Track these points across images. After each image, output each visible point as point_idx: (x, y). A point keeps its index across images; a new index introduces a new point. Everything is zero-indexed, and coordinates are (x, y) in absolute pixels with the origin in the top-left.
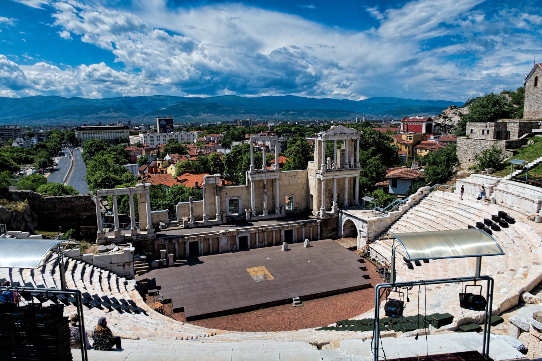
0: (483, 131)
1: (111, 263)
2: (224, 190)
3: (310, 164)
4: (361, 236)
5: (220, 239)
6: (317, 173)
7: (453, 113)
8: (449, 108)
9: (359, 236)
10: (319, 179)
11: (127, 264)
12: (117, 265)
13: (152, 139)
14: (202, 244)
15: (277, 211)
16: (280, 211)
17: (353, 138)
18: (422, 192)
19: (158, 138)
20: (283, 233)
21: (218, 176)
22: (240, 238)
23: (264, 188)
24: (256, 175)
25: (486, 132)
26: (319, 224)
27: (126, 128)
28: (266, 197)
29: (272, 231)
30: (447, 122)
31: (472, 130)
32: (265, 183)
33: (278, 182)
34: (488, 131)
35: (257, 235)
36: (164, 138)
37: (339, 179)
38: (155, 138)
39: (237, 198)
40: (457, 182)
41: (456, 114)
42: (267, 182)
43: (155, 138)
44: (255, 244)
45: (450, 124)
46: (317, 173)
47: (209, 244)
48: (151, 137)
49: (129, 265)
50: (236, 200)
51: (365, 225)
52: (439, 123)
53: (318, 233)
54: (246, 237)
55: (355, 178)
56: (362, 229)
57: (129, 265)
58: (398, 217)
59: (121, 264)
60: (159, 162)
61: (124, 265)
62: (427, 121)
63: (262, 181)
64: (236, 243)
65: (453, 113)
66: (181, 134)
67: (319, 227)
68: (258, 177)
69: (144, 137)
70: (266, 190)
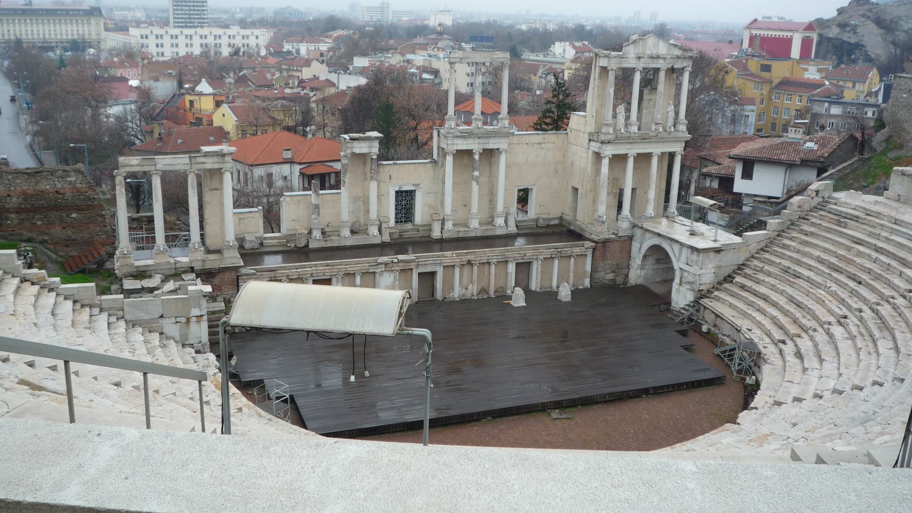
1: (162, 316)
2: (387, 169)
3: (576, 120)
4: (684, 280)
5: (377, 275)
6: (590, 140)
7: (863, 16)
9: (677, 280)
10: (598, 156)
11: (194, 319)
12: (173, 320)
13: (160, 41)
15: (500, 221)
16: (506, 222)
17: (678, 65)
18: (817, 192)
19: (175, 41)
20: (512, 268)
21: (377, 138)
23: (474, 169)
26: (589, 253)
27: (94, 12)
28: (475, 187)
29: (489, 263)
32: (477, 157)
33: (503, 158)
35: (457, 271)
36: (188, 41)
37: (638, 154)
38: (167, 41)
39: (412, 188)
40: (893, 176)
41: (869, 18)
42: (480, 154)
43: (167, 41)
44: (452, 288)
45: (853, 41)
46: (590, 140)
48: (157, 37)
49: (198, 322)
50: (411, 192)
52: (830, 35)
53: (585, 271)
54: (433, 274)
55: (672, 155)
56: (685, 267)
57: (198, 322)
58: (763, 244)
59: (183, 320)
60: (191, 98)
61: (188, 321)
63: (469, 152)
65: (863, 16)
66: (230, 32)
67: (589, 260)
68: (463, 145)
69: (142, 37)
70: (476, 173)
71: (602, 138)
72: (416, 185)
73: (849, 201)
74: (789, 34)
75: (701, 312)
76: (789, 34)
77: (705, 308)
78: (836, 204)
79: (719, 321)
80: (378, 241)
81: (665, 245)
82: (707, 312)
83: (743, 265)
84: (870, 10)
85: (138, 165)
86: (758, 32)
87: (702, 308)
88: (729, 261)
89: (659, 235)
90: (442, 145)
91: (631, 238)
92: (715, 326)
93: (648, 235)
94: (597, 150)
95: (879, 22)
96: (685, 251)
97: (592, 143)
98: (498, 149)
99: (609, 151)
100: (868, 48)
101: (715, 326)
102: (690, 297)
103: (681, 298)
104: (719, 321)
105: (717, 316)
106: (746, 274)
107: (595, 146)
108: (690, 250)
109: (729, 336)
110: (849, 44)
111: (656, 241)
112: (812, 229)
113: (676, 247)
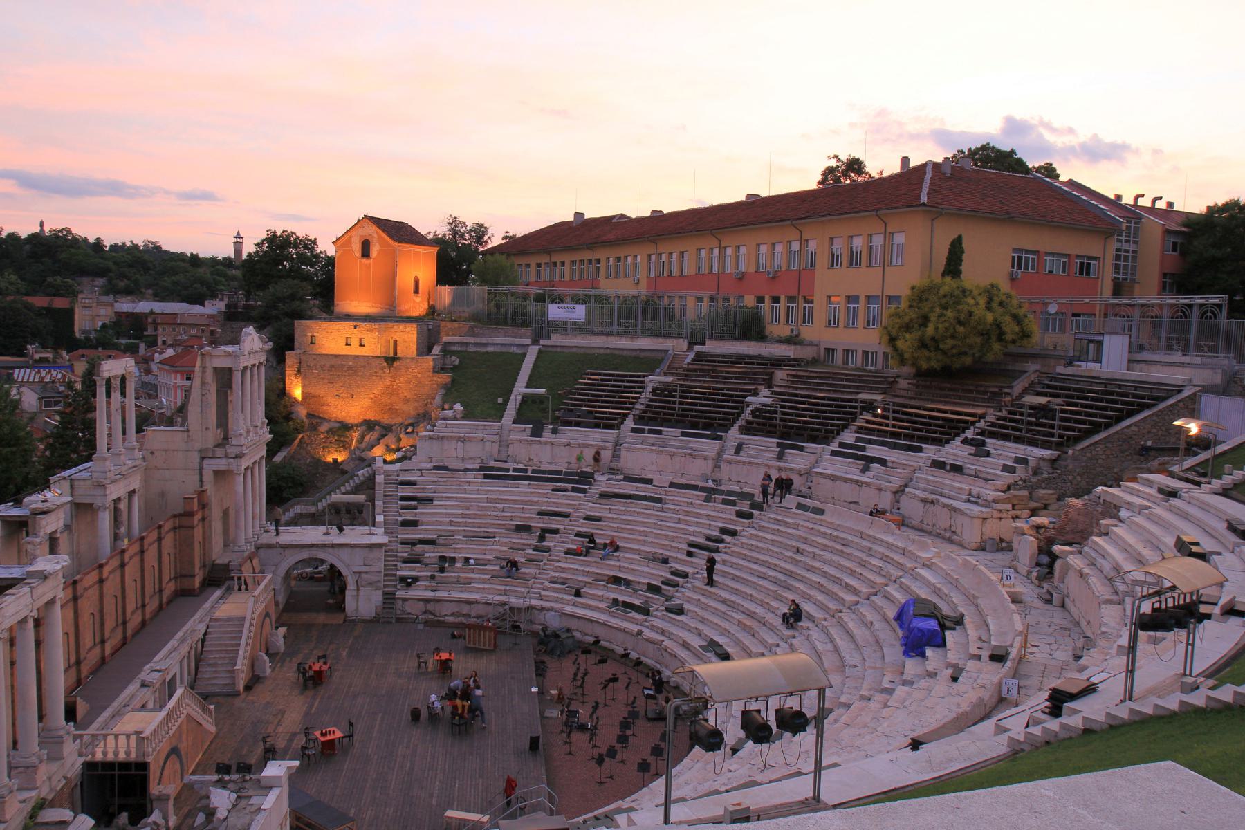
6: (203, 458)
33: (136, 499)
46: (203, 458)
56: (364, 569)
71: (232, 451)
77: (405, 600)
79: (430, 607)
81: (320, 554)
87: (400, 602)
89: (313, 545)
92: (426, 612)
93: (287, 552)
94: (223, 468)
96: (359, 555)
97: (206, 462)
102: (378, 597)
104: (430, 607)
105: (427, 601)
107: (221, 464)
109: (452, 614)
111: (306, 555)
113: (344, 554)
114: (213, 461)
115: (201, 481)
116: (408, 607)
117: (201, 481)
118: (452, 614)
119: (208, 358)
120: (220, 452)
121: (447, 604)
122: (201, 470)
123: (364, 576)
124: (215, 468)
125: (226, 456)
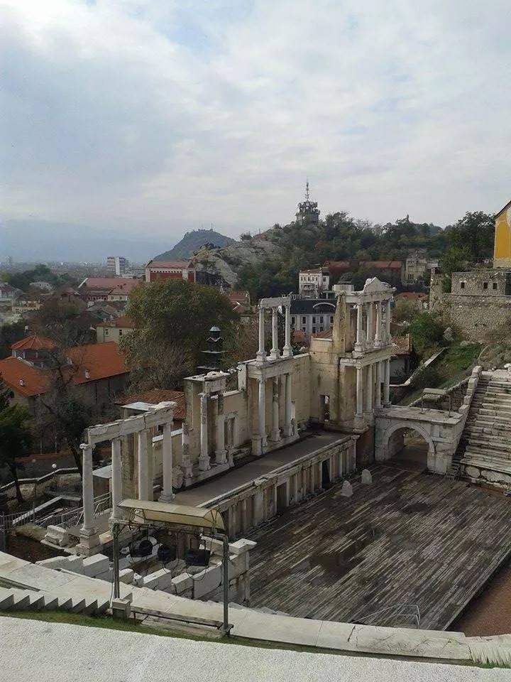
0: (486, 286)
7: (216, 255)
8: (204, 248)
9: (432, 450)
14: (234, 514)
20: (321, 464)
22: (279, 488)
24: (268, 370)
25: (490, 286)
30: (209, 271)
31: (463, 284)
33: (290, 379)
34: (495, 286)
41: (219, 256)
45: (214, 273)
46: (340, 358)
47: (242, 511)
51: (448, 431)
62: (189, 267)
64: (272, 501)
72: (235, 413)
73: (502, 377)
74: (180, 270)
75: (462, 470)
76: (180, 270)
77: (466, 466)
78: (490, 380)
80: (227, 467)
81: (412, 426)
82: (468, 468)
83: (464, 431)
84: (218, 251)
85: (106, 433)
86: (156, 270)
88: (460, 428)
90: (251, 376)
91: (375, 427)
94: (350, 365)
95: (226, 259)
96: (437, 428)
98: (287, 375)
99: (359, 365)
100: (225, 278)
101: (481, 477)
102: (448, 461)
103: (439, 463)
104: (483, 473)
105: (481, 469)
106: (474, 436)
108: (442, 427)
109: (498, 482)
110: (212, 275)
111: (404, 425)
112: (493, 399)
113: (428, 427)
114: (346, 360)
115: (339, 372)
116: (470, 471)
117: (339, 372)
118: (498, 482)
119: (343, 297)
120: (348, 355)
121: (495, 473)
122: (339, 365)
123: (439, 444)
124: (346, 364)
125: (352, 358)
